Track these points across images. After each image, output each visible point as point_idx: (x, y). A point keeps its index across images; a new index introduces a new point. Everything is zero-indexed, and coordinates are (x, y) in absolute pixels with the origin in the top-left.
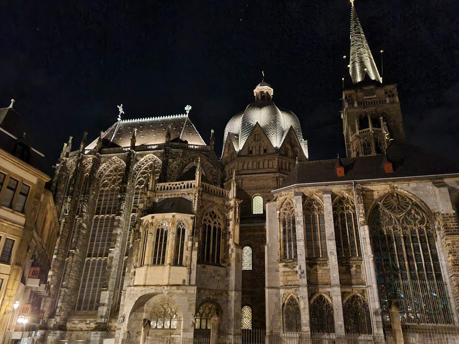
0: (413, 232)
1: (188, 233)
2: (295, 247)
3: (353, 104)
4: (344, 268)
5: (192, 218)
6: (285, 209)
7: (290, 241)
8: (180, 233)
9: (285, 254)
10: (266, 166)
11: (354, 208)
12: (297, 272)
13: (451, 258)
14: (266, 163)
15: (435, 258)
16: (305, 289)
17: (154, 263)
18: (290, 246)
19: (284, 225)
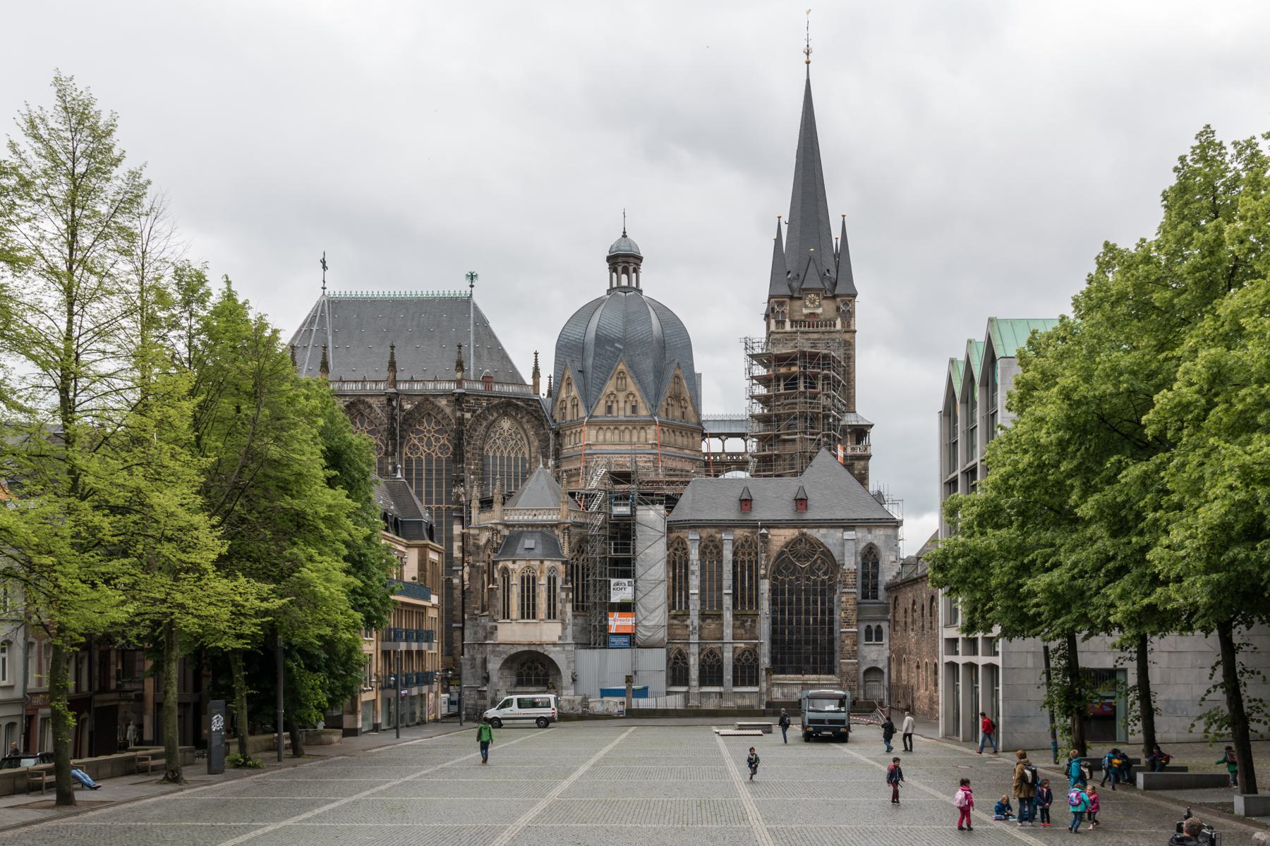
0: (815, 583)
1: (559, 582)
2: (687, 597)
3: (783, 323)
4: (738, 623)
5: (563, 563)
6: (676, 549)
7: (680, 589)
8: (552, 581)
9: (674, 603)
10: (635, 439)
11: (757, 554)
12: (687, 626)
13: (843, 615)
14: (635, 431)
15: (831, 612)
16: (696, 646)
17: (523, 617)
18: (680, 595)
19: (674, 570)
